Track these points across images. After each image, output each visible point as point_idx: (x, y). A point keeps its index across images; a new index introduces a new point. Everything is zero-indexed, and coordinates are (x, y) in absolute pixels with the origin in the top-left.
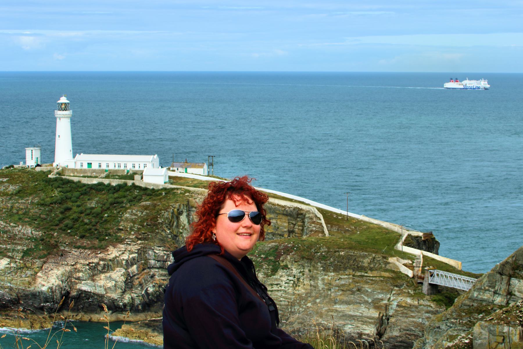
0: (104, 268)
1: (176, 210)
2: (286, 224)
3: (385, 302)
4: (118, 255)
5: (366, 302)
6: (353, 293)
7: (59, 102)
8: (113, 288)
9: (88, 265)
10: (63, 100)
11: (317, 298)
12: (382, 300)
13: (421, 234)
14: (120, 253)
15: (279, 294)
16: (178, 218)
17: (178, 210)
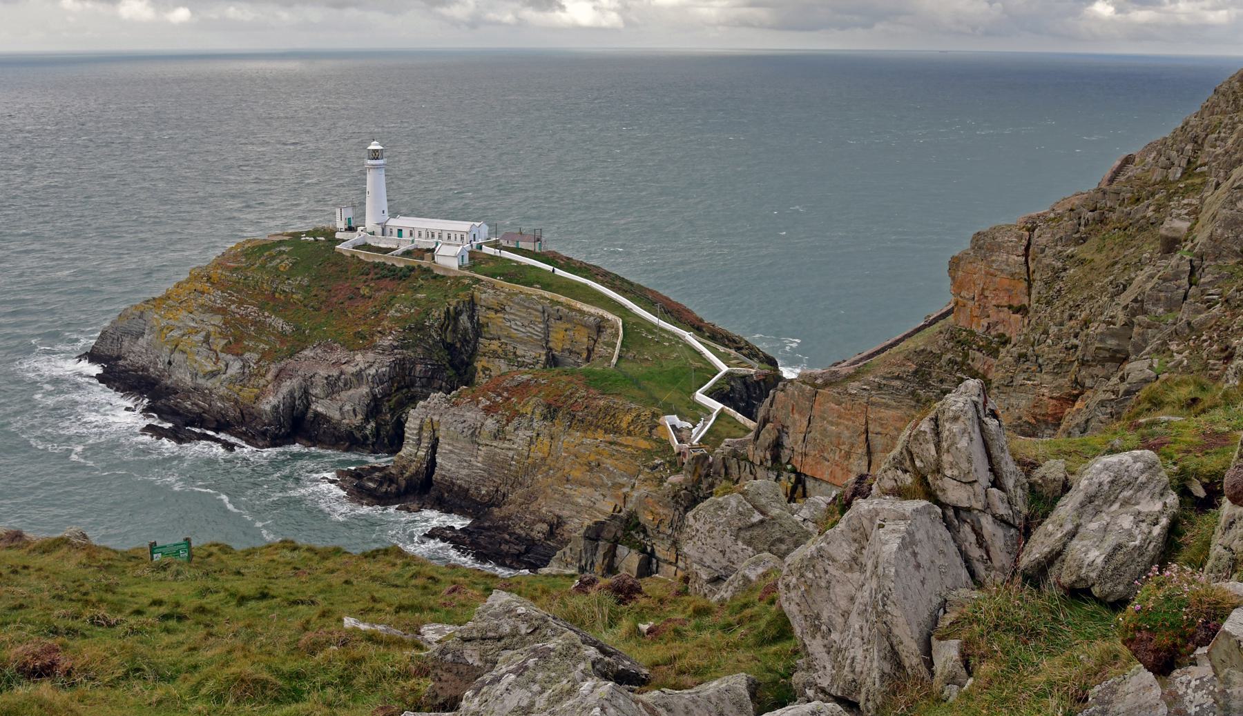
0: (345, 385)
1: (451, 308)
2: (586, 340)
3: (625, 490)
4: (363, 367)
5: (603, 485)
6: (591, 470)
7: (370, 148)
8: (351, 413)
9: (326, 378)
10: (375, 146)
11: (550, 469)
12: (623, 486)
13: (753, 371)
14: (366, 365)
15: (511, 454)
16: (456, 319)
17: (455, 308)
